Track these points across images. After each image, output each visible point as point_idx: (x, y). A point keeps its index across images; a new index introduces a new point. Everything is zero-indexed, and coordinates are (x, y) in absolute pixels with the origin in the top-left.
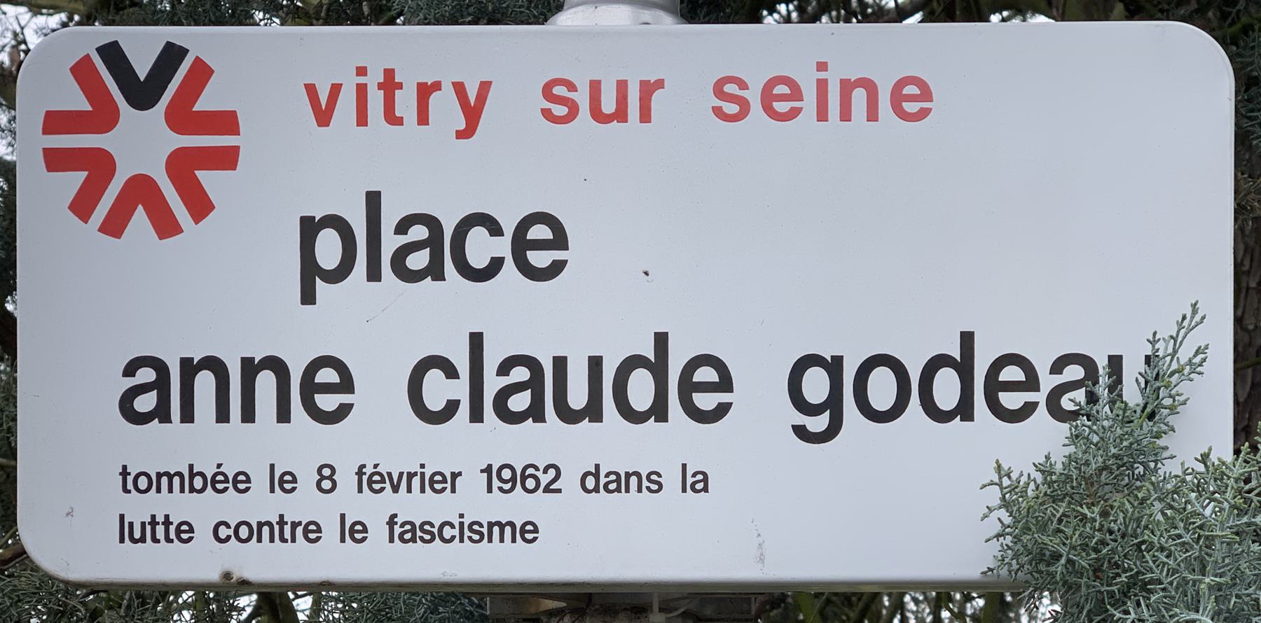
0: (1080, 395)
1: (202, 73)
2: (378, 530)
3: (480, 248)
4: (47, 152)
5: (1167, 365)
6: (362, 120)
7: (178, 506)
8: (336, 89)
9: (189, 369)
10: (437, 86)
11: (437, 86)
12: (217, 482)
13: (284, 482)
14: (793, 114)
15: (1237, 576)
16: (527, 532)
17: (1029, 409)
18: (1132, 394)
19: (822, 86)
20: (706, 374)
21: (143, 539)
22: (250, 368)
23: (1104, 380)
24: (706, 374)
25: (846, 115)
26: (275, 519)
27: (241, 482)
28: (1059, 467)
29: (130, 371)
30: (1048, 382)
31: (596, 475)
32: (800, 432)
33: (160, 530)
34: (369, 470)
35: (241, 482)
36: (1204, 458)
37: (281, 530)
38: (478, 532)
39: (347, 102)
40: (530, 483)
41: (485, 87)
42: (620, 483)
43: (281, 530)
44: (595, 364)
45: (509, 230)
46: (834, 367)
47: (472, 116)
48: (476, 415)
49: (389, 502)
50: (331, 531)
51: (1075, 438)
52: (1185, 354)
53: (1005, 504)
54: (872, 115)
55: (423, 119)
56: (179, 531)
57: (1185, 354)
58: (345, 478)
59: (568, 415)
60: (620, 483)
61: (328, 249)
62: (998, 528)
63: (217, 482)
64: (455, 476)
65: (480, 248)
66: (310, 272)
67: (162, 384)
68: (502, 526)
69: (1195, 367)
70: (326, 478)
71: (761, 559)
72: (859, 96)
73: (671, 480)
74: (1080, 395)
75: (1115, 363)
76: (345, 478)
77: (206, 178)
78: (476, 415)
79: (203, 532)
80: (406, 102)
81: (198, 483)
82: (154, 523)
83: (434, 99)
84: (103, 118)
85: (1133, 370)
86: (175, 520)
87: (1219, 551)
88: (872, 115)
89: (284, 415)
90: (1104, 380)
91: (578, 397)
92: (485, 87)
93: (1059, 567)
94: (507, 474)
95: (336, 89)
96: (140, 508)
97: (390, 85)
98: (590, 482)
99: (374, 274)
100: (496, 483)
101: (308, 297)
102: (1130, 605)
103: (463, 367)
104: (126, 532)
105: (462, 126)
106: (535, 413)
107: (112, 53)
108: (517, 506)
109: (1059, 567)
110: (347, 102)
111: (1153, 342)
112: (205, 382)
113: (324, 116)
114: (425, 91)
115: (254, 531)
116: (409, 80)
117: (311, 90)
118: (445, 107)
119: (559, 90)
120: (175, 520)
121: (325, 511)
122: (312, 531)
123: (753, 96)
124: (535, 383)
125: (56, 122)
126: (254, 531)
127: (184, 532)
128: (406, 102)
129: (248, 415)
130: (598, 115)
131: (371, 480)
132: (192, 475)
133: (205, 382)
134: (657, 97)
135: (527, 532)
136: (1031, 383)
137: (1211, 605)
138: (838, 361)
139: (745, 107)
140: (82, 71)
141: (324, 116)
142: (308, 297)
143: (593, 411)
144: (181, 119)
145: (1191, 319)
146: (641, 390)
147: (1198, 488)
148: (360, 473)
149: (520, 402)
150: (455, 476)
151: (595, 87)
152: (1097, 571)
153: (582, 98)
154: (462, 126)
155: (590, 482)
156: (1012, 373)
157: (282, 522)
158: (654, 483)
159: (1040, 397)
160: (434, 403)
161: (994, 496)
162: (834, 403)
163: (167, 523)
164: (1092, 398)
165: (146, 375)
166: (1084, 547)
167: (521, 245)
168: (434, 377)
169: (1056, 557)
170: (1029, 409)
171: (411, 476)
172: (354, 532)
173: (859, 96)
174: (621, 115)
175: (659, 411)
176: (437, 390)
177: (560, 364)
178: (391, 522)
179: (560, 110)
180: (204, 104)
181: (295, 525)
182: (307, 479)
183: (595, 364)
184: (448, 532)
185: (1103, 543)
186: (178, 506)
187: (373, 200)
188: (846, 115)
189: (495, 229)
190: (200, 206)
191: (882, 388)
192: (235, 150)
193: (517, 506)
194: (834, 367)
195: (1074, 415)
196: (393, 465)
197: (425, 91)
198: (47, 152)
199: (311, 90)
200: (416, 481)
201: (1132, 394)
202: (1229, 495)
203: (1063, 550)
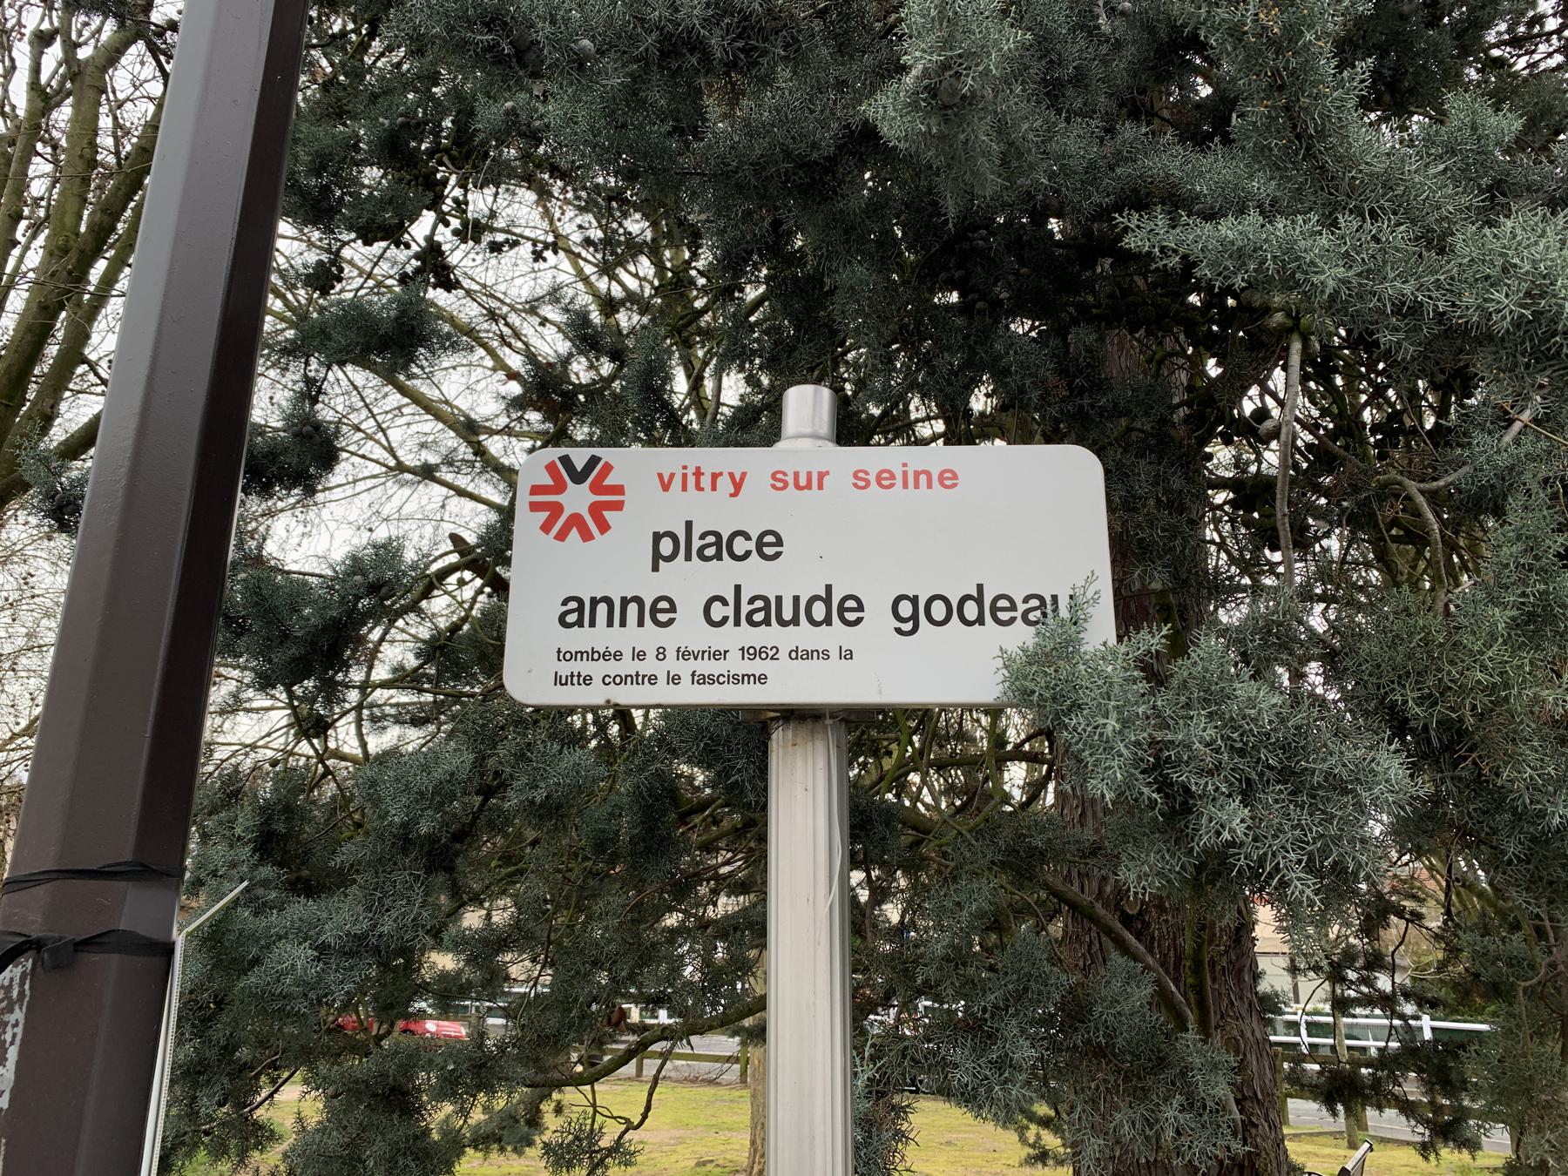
0: (1038, 613)
1: (608, 468)
2: (686, 679)
3: (740, 546)
4: (556, 538)
5: (1080, 600)
6: (684, 488)
7: (584, 667)
8: (672, 476)
9: (594, 602)
10: (721, 474)
11: (721, 474)
12: (605, 656)
13: (639, 655)
14: (892, 486)
15: (1127, 701)
16: (762, 679)
17: (1013, 620)
18: (1064, 613)
19: (905, 474)
20: (851, 604)
21: (566, 684)
22: (625, 602)
23: (1049, 608)
24: (851, 604)
25: (917, 486)
26: (634, 674)
27: (618, 656)
28: (1031, 648)
29: (565, 603)
30: (1021, 607)
31: (797, 652)
32: (899, 631)
33: (575, 679)
34: (682, 650)
35: (618, 656)
36: (1105, 644)
37: (637, 679)
38: (737, 679)
39: (677, 481)
40: (764, 655)
41: (744, 475)
42: (808, 655)
43: (637, 679)
44: (796, 599)
45: (754, 539)
46: (914, 601)
47: (738, 486)
48: (737, 623)
49: (692, 665)
50: (662, 678)
51: (1038, 634)
52: (1089, 594)
53: (1006, 667)
54: (930, 486)
55: (714, 488)
56: (585, 680)
57: (1089, 594)
58: (671, 654)
59: (783, 623)
60: (808, 655)
61: (666, 547)
62: (1002, 678)
63: (605, 656)
64: (726, 652)
65: (740, 546)
66: (657, 557)
67: (580, 610)
68: (749, 676)
69: (1095, 601)
70: (661, 654)
71: (880, 692)
72: (923, 478)
73: (834, 654)
74: (1038, 613)
75: (1055, 598)
76: (671, 654)
77: (608, 515)
78: (737, 623)
79: (597, 681)
80: (706, 481)
81: (596, 656)
82: (572, 676)
83: (719, 480)
84: (559, 488)
85: (1063, 603)
86: (583, 674)
87: (1116, 689)
88: (930, 486)
89: (641, 623)
90: (1049, 608)
91: (787, 614)
92: (744, 475)
93: (1035, 698)
94: (752, 651)
95: (672, 476)
96: (565, 669)
97: (698, 473)
98: (794, 655)
99: (688, 558)
100: (746, 655)
101: (655, 568)
102: (1073, 716)
103: (731, 601)
104: (558, 680)
105: (732, 491)
106: (767, 622)
107: (566, 460)
108: (757, 666)
109: (1035, 698)
110: (677, 481)
111: (1073, 589)
112: (602, 609)
113: (666, 487)
114: (715, 476)
115: (623, 680)
116: (707, 473)
117: (660, 476)
118: (725, 484)
119: (779, 476)
120: (583, 674)
121: (660, 670)
122: (652, 679)
123: (872, 478)
124: (767, 608)
125: (536, 490)
126: (623, 680)
127: (587, 680)
128: (706, 481)
129: (623, 624)
130: (798, 487)
131: (683, 654)
132: (593, 653)
133: (602, 609)
134: (826, 479)
135: (762, 679)
136: (1013, 607)
137: (1115, 716)
138: (916, 597)
139: (868, 483)
140: (551, 468)
141: (666, 487)
142: (655, 568)
143: (795, 621)
144: (597, 488)
145: (1091, 578)
146: (819, 611)
147: (1103, 658)
148: (678, 651)
149: (759, 617)
150: (726, 652)
151: (796, 475)
152: (1054, 699)
153: (790, 479)
154: (732, 491)
155: (794, 655)
156: (1003, 603)
157: (637, 675)
158: (826, 655)
159: (1018, 614)
160: (716, 617)
161: (1000, 663)
162: (915, 617)
163: (579, 676)
164: (1044, 615)
165: (573, 605)
166: (1047, 687)
167: (760, 545)
168: (716, 605)
169: (1033, 692)
170: (1013, 620)
171: (704, 652)
172: (674, 679)
173: (923, 478)
174: (809, 486)
175: (828, 621)
176: (717, 611)
177: (779, 599)
178: (693, 675)
179: (780, 485)
180: (608, 482)
181: (644, 676)
182: (651, 654)
183: (796, 599)
184: (721, 679)
185: (1056, 685)
186: (584, 667)
187: (689, 525)
188: (917, 486)
189: (748, 538)
190: (604, 527)
191: (938, 610)
192: (623, 502)
193: (757, 666)
194: (914, 601)
195: (1035, 623)
196: (695, 647)
197: (715, 476)
198: (556, 538)
199: (660, 476)
200: (706, 655)
201: (1064, 613)
202: (1120, 661)
203: (1037, 689)
